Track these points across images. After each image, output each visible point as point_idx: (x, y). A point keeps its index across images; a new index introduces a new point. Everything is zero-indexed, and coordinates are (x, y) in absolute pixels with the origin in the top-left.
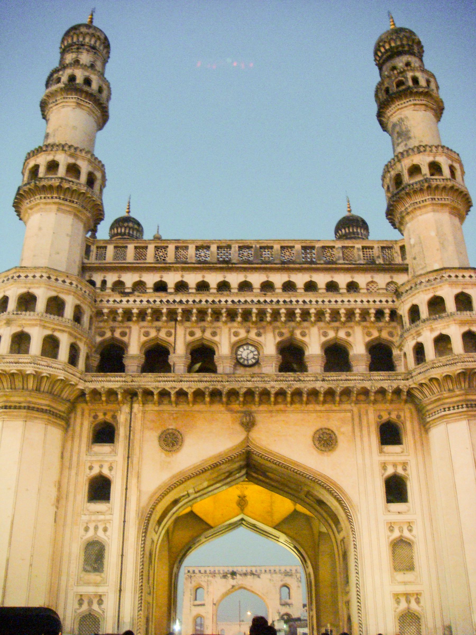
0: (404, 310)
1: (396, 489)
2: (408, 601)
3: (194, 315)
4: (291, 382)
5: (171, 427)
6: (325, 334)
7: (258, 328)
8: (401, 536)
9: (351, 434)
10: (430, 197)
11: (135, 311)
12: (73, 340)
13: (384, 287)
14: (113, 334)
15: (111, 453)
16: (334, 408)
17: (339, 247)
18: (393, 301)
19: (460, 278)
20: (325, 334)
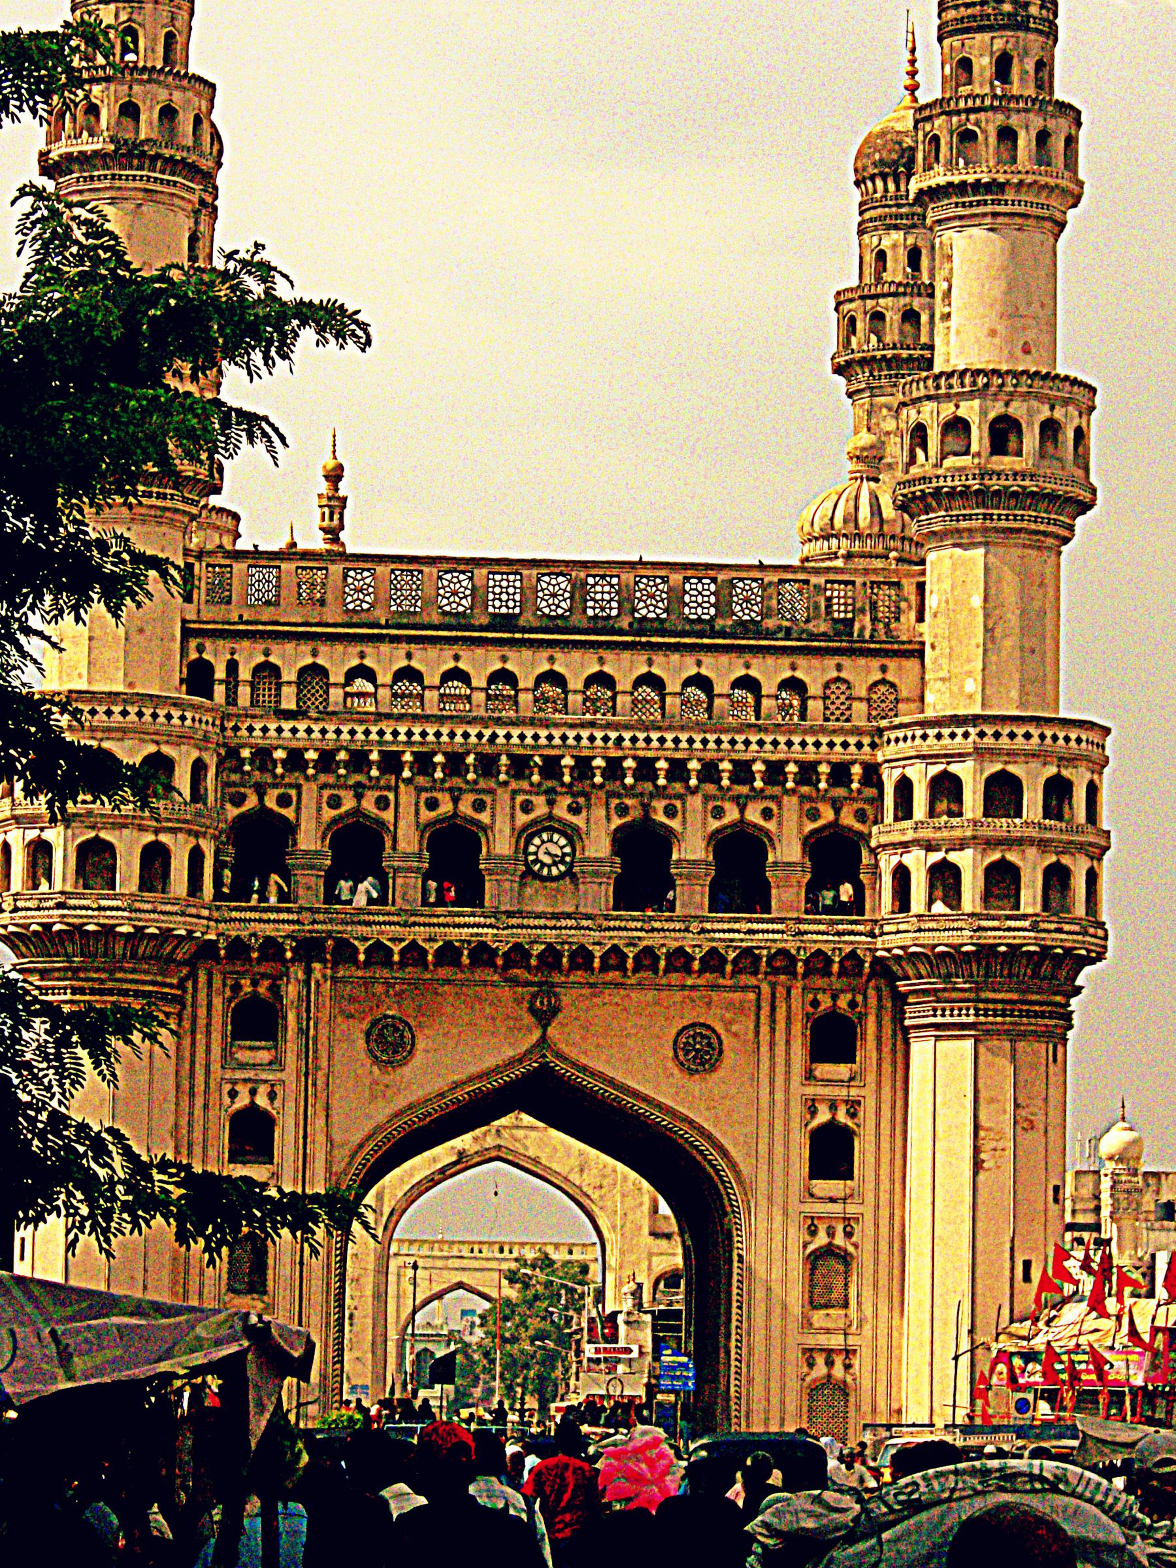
0: (889, 778)
1: (831, 1153)
2: (830, 1364)
3: (439, 769)
4: (635, 934)
5: (390, 1013)
6: (718, 813)
7: (574, 795)
8: (830, 1244)
9: (751, 1035)
10: (982, 511)
11: (311, 755)
12: (192, 842)
13: (863, 693)
14: (261, 800)
15: (270, 1063)
16: (721, 981)
17: (770, 583)
18: (873, 746)
19: (1004, 741)
20: (718, 813)
